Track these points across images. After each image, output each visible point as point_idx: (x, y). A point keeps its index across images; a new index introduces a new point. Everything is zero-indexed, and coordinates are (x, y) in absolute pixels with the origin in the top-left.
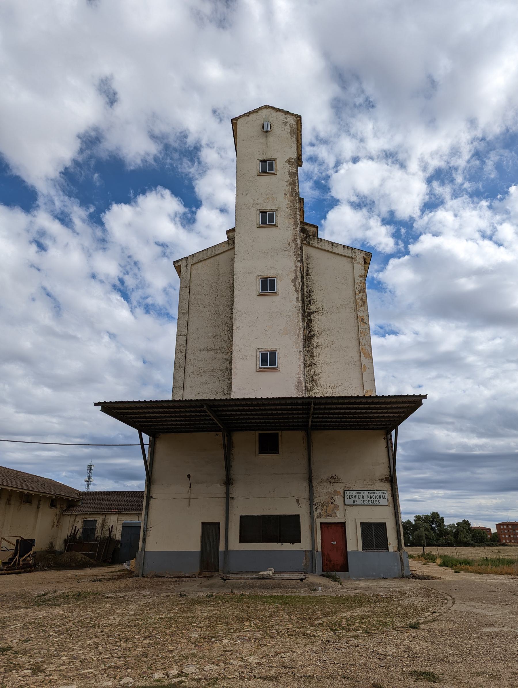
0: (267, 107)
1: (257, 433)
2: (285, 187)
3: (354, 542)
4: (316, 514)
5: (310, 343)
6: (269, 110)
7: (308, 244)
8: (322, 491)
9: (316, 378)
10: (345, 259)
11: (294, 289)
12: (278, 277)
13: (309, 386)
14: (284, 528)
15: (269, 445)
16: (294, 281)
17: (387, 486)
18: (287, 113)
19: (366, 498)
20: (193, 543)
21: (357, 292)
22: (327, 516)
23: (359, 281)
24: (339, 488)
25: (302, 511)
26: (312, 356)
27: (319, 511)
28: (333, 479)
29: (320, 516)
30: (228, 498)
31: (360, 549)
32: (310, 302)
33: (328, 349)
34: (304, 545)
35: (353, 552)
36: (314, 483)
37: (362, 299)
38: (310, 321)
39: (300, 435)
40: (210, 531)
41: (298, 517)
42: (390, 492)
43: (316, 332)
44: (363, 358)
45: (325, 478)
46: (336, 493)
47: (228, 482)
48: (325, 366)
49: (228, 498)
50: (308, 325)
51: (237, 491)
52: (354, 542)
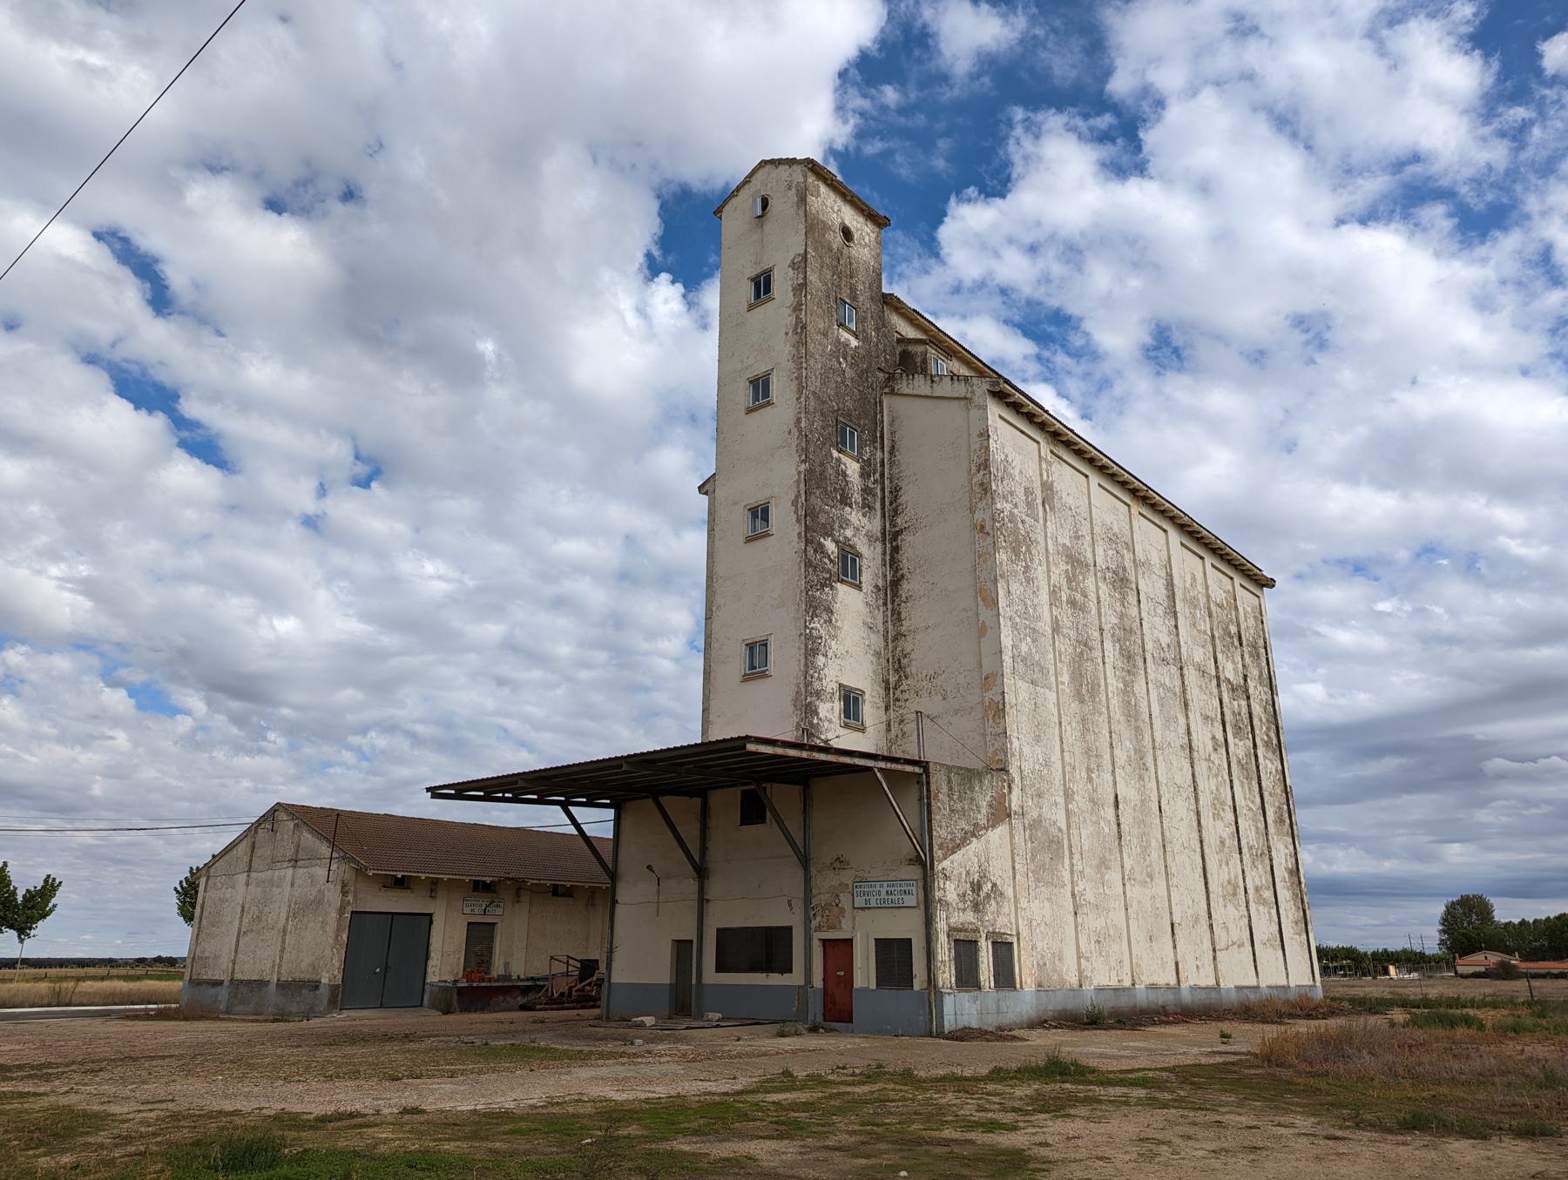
0: (764, 163)
1: (738, 791)
2: (788, 319)
3: (864, 973)
4: (814, 923)
5: (895, 595)
6: (768, 167)
7: (893, 393)
8: (824, 883)
9: (905, 661)
10: (956, 403)
11: (794, 517)
12: (773, 501)
13: (892, 679)
14: (764, 949)
15: (753, 811)
16: (795, 502)
17: (916, 872)
18: (791, 162)
19: (883, 895)
20: (661, 974)
21: (974, 469)
22: (829, 928)
23: (977, 446)
24: (847, 877)
25: (794, 920)
26: (899, 620)
27: (819, 918)
28: (840, 863)
29: (819, 929)
30: (702, 901)
31: (873, 986)
32: (896, 510)
33: (924, 600)
34: (795, 978)
35: (866, 990)
36: (813, 871)
37: (982, 484)
38: (896, 549)
39: (796, 790)
40: (683, 951)
41: (790, 928)
42: (920, 884)
43: (905, 571)
44: (982, 608)
45: (828, 862)
46: (843, 886)
47: (701, 873)
48: (919, 637)
49: (702, 901)
50: (892, 559)
51: (715, 888)
52: (864, 973)
